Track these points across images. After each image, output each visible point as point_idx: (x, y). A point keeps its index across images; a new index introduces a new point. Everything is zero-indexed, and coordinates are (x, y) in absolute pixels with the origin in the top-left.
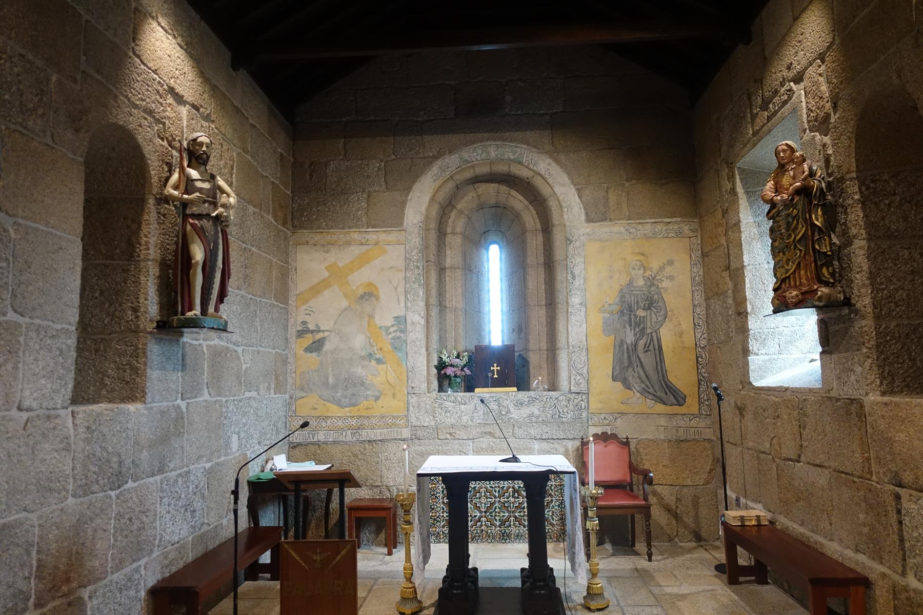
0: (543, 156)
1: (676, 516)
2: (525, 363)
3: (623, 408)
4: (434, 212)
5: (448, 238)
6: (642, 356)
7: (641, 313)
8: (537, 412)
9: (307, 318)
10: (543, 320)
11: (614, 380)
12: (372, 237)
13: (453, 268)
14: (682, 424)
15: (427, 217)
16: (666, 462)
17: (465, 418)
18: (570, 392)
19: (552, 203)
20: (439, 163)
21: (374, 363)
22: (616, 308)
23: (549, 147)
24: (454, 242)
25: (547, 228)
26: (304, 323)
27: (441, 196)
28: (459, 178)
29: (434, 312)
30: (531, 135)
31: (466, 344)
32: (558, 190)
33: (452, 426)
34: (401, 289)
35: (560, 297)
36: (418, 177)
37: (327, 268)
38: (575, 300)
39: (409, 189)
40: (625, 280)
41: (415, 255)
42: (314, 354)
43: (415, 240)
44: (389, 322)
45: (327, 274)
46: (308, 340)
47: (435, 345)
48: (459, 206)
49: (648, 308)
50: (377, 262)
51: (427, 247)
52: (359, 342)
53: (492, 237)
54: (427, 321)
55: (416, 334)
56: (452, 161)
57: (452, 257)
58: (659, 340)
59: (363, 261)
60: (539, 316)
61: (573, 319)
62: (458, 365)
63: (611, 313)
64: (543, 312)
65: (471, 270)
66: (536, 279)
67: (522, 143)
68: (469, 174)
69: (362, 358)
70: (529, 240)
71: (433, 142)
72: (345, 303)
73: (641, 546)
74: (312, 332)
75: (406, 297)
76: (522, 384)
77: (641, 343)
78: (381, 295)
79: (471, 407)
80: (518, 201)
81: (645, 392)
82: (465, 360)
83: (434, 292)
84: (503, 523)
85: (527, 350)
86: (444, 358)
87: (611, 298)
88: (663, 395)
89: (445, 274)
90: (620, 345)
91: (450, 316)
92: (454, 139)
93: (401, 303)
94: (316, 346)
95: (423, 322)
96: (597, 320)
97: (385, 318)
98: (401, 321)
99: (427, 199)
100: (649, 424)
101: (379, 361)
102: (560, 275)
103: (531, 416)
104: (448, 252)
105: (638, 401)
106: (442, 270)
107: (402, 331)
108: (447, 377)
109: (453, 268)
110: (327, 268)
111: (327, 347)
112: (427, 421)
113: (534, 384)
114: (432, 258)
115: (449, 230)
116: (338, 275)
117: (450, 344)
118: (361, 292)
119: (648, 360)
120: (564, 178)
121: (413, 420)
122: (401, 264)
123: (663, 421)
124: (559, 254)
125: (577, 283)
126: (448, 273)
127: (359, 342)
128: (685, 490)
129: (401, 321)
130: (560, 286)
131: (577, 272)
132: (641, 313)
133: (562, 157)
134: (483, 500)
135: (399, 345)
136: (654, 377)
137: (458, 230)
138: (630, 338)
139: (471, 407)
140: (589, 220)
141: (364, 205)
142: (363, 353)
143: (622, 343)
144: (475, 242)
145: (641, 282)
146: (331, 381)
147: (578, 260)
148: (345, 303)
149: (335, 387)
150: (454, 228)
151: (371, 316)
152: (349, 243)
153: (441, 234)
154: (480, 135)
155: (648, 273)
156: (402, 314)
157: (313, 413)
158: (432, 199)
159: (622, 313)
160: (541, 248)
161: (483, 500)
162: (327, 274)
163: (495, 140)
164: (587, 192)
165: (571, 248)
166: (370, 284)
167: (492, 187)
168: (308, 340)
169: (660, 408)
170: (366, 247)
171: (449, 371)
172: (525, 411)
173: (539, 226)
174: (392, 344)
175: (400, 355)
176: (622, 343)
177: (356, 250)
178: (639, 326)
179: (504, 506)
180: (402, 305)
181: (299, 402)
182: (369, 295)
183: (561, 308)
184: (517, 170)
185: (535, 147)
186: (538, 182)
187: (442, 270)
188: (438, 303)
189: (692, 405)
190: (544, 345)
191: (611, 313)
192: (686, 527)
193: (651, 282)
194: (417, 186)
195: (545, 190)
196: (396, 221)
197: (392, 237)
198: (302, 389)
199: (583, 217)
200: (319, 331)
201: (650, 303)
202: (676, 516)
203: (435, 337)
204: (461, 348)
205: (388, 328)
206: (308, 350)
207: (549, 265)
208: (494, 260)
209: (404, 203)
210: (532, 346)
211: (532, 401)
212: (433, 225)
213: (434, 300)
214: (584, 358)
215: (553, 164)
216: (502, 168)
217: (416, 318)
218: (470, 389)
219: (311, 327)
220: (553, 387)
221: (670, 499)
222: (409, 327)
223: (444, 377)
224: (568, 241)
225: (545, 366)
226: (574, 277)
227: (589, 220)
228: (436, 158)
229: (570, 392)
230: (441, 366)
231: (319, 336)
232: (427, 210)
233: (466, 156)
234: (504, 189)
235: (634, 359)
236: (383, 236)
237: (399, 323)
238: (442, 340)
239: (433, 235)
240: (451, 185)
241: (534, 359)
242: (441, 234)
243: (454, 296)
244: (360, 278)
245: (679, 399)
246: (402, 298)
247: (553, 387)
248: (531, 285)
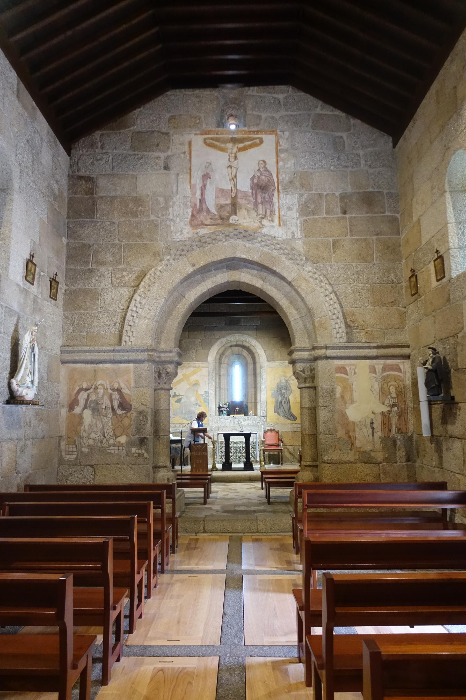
0: (253, 339)
1: (293, 455)
2: (247, 407)
3: (277, 421)
4: (218, 357)
5: (222, 365)
6: (284, 405)
7: (283, 391)
8: (250, 422)
9: (176, 391)
10: (253, 393)
11: (275, 412)
12: (197, 365)
13: (224, 375)
14: (295, 426)
15: (215, 358)
16: (290, 438)
17: (227, 424)
18: (261, 416)
19: (256, 355)
20: (220, 340)
21: (198, 406)
22: (276, 389)
23: (255, 336)
24: (224, 366)
25: (254, 363)
26: (175, 393)
27: (220, 352)
28: (226, 346)
29: (218, 390)
30: (249, 332)
31: (228, 400)
32: (258, 350)
33: (223, 427)
34: (207, 382)
35: (258, 385)
36: (212, 345)
37: (183, 375)
38: (263, 387)
39: (210, 349)
40: (279, 380)
41: (211, 371)
42: (178, 403)
43: (212, 366)
44: (203, 393)
45: (182, 377)
46: (176, 398)
47: (218, 401)
48: (226, 354)
49: (286, 389)
50: (199, 373)
51: (215, 369)
52: (193, 399)
53: (236, 363)
54: (215, 393)
55: (212, 397)
56: (224, 340)
57: (223, 371)
58: (289, 400)
59: (194, 373)
60: (251, 391)
61: (262, 393)
62: (225, 407)
63: (274, 391)
64: (253, 390)
65: (229, 375)
66: (251, 379)
67: (247, 335)
68: (229, 345)
69: (194, 405)
70: (249, 366)
71: (217, 334)
72: (188, 387)
73: (280, 464)
74: (177, 396)
75: (209, 385)
76: (246, 414)
77: (283, 401)
78: (201, 385)
79: (229, 421)
80: (245, 353)
81: (284, 416)
82: (227, 406)
83: (217, 383)
84: (239, 457)
85: (248, 403)
86: (221, 405)
87: (274, 386)
88: (290, 417)
89: (220, 376)
90: (277, 401)
91: (222, 391)
92: (224, 333)
93: (207, 388)
94: (179, 401)
95: (214, 393)
96: (270, 393)
97: (201, 392)
98: (207, 393)
99: (215, 353)
100: (285, 426)
101: (199, 406)
102: (258, 379)
103: (248, 424)
104: (222, 370)
105: (282, 419)
106: (220, 376)
107: (207, 396)
108: (222, 411)
109: (224, 375)
110: (183, 375)
111: (183, 401)
112: (215, 425)
113: (250, 414)
114: (217, 372)
115: (222, 362)
116: (186, 377)
117: (222, 400)
118: (194, 383)
119: (285, 406)
120: (260, 347)
121: (210, 425)
122: (207, 374)
123: (289, 425)
124: (258, 371)
125: (264, 381)
126: (222, 377)
127: (193, 399)
128: (296, 447)
129: (207, 393)
130: (258, 382)
131: (264, 377)
132: (283, 391)
133: (260, 340)
134: (233, 450)
135: (206, 400)
136: (287, 411)
137: (226, 362)
138: (280, 399)
139: (229, 421)
140: (268, 361)
141: (195, 354)
142: (195, 403)
143: (277, 400)
144: (230, 365)
145: (284, 381)
146: (184, 412)
147: (264, 374)
148: (188, 387)
149: (185, 414)
150: (224, 361)
151: (197, 391)
152: (189, 367)
153: (220, 363)
154: (234, 332)
155: (286, 378)
156: (207, 390)
157: (178, 422)
158: (217, 353)
159: (277, 391)
160: (253, 369)
161: (233, 450)
162: (182, 377)
163: (237, 333)
164: (267, 352)
165: (262, 370)
166: (197, 381)
167: (237, 348)
168: (176, 398)
169: (289, 421)
170: (195, 368)
171: (222, 409)
172: (247, 422)
173: (252, 362)
174: (204, 400)
175: (206, 403)
176: (277, 400)
177: (192, 369)
178: (283, 395)
179: (239, 452)
180: (207, 387)
181: (173, 419)
182: (196, 384)
183: (258, 389)
184: (245, 344)
185: (251, 336)
186: (251, 348)
187: (220, 376)
188: (219, 387)
189: (299, 420)
190: (253, 401)
191: (274, 391)
192: (296, 458)
193: (287, 381)
194: (212, 348)
195: (254, 351)
196: (206, 360)
197: (204, 365)
198: (174, 415)
199: (266, 360)
200: (180, 396)
201: (287, 388)
202: (293, 455)
203: (218, 398)
204: (226, 402)
205: (202, 395)
206: (176, 402)
207: (255, 375)
208: (237, 371)
209: (208, 354)
210: (249, 401)
211: (249, 419)
212: (217, 361)
213: (217, 386)
214: (265, 405)
215: (257, 342)
216: (240, 343)
217: (212, 392)
218: (228, 414)
219: (177, 394)
220: (256, 414)
221: (291, 450)
222: (210, 395)
223: (220, 412)
224: (261, 367)
225: (253, 408)
226: (263, 379)
227: (268, 361)
228: (219, 339)
229: (261, 416)
230: (220, 407)
231: (180, 397)
232: (216, 356)
233: (228, 338)
234: (241, 348)
235: (281, 406)
236: (201, 365)
237: (206, 393)
238: (220, 399)
239: (217, 364)
240: (223, 348)
241: (250, 405)
242: (220, 363)
243: (224, 385)
244: (193, 379)
245: (295, 419)
246: (207, 385)
247: (256, 414)
248: (249, 381)
